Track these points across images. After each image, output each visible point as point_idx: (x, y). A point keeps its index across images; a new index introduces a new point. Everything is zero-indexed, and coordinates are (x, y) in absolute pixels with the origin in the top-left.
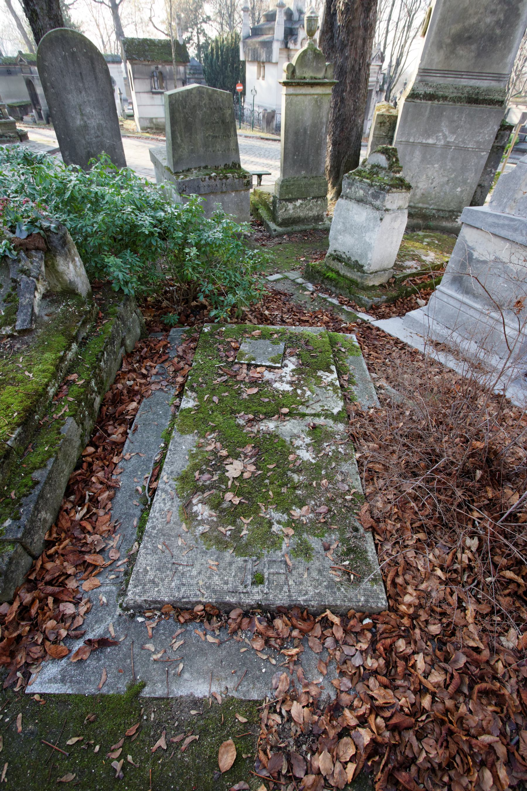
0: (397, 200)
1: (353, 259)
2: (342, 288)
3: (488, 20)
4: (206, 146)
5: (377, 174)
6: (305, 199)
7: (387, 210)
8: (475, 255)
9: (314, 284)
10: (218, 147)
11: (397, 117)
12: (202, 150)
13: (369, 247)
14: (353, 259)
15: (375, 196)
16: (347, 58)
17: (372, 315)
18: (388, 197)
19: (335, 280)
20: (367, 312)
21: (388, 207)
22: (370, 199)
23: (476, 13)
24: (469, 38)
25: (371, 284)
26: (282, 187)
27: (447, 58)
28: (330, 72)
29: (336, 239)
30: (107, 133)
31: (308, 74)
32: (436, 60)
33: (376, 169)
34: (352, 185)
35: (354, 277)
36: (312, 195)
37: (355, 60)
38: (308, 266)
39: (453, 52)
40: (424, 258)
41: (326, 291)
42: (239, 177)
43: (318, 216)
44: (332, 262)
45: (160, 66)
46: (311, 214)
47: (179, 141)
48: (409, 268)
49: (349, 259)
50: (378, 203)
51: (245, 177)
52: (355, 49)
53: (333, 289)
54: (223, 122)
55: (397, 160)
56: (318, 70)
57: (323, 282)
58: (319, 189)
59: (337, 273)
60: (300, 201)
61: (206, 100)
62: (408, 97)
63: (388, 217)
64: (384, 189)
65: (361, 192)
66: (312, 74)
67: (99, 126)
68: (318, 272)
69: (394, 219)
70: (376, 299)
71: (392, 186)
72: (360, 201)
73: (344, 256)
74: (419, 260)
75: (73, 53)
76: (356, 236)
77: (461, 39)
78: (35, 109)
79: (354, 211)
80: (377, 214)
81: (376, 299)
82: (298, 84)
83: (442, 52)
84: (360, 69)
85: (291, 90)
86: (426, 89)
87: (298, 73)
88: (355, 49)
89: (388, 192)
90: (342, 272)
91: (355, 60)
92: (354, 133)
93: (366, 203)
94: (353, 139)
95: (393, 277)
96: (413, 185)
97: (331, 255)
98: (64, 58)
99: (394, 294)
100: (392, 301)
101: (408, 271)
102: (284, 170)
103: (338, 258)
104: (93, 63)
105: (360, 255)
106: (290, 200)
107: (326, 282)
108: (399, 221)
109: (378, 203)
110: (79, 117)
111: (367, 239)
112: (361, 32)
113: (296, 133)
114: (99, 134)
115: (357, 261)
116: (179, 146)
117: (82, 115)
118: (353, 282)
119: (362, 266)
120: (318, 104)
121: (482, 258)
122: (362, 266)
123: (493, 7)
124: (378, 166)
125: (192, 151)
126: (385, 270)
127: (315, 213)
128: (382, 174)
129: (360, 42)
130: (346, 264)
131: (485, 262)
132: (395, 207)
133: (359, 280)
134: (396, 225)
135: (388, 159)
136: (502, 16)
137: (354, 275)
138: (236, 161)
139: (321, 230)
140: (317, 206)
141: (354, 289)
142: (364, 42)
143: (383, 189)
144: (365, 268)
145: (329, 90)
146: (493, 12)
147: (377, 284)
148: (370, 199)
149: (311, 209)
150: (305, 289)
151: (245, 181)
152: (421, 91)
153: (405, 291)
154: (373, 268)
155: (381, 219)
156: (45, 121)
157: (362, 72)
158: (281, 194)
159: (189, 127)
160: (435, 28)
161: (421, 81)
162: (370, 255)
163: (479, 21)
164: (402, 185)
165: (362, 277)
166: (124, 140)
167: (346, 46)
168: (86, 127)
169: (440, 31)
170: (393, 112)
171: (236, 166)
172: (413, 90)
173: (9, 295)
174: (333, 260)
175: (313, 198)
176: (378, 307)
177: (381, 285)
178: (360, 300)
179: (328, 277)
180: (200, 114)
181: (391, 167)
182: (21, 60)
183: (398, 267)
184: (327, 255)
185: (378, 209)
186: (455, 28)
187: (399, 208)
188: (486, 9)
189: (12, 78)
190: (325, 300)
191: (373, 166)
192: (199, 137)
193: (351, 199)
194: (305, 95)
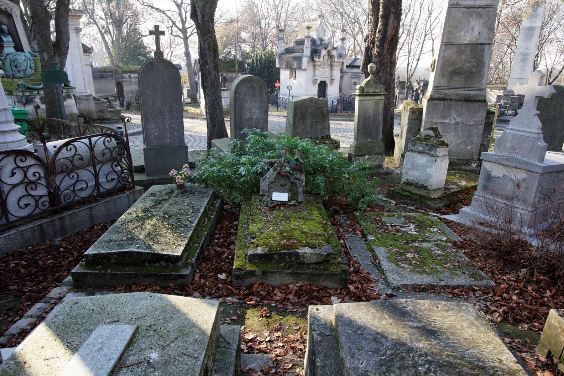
0: (442, 151)
1: (420, 183)
2: (415, 200)
3: (468, 65)
4: (312, 126)
5: (429, 139)
6: (370, 155)
7: (438, 156)
8: (493, 174)
9: (395, 200)
10: (318, 127)
11: (422, 109)
12: (309, 129)
13: (430, 176)
14: (420, 183)
15: (430, 150)
16: (381, 77)
17: (438, 213)
18: (438, 150)
19: (409, 196)
20: (434, 212)
21: (438, 155)
22: (427, 151)
23: (460, 63)
24: (459, 72)
25: (433, 197)
26: (356, 148)
27: (448, 81)
28: (383, 89)
29: (407, 173)
30: (261, 121)
31: (371, 90)
32: (442, 82)
33: (427, 137)
34: (415, 145)
35: (423, 194)
36: (375, 152)
37: (386, 78)
38: (389, 190)
39: (451, 78)
40: (460, 184)
41: (405, 203)
42: (333, 143)
43: (379, 165)
44: (406, 187)
45: (224, 74)
46: (375, 164)
47: (297, 124)
48: (453, 189)
49: (417, 183)
50: (432, 153)
51: (336, 143)
52: (386, 73)
53: (409, 202)
54: (322, 114)
55: (439, 133)
56: (377, 88)
57: (401, 198)
58: (379, 149)
59: (410, 192)
60: (367, 156)
61: (314, 103)
62: (429, 100)
63: (439, 160)
64: (434, 147)
65: (421, 148)
66: (373, 90)
67: (258, 117)
68: (397, 193)
69: (442, 161)
70: (439, 205)
71: (439, 145)
72: (420, 152)
73: (413, 182)
74: (457, 185)
75: (253, 86)
76: (421, 171)
77: (456, 73)
78: (119, 100)
79: (418, 158)
80: (433, 158)
81: (439, 205)
82: (366, 95)
83: (445, 79)
84: (389, 83)
85: (362, 98)
86: (439, 96)
87: (365, 90)
88: (386, 73)
89: (437, 147)
90: (413, 192)
91: (386, 78)
92: (389, 116)
93: (425, 153)
94: (389, 120)
95: (445, 193)
96: (449, 143)
97: (404, 183)
98: (248, 88)
99: (448, 202)
100: (448, 206)
101: (453, 190)
102: (357, 138)
103: (409, 184)
104: (261, 89)
105: (425, 181)
106: (361, 156)
107: (403, 198)
108: (444, 162)
109: (432, 153)
110: (249, 114)
111: (428, 172)
112: (389, 65)
113: (365, 119)
114: (257, 121)
115: (422, 184)
116: (297, 127)
117: (250, 112)
118: (421, 196)
119: (427, 187)
120: (377, 104)
121: (497, 176)
122: (427, 187)
123: (469, 60)
124: (429, 136)
125: (304, 129)
126: (440, 189)
127: (377, 163)
128: (432, 139)
129: (388, 69)
130: (416, 187)
131: (499, 177)
132: (441, 155)
133: (426, 195)
134: (443, 164)
135: (434, 132)
136: (475, 64)
137: (423, 192)
138: (328, 134)
139: (382, 173)
140: (378, 159)
141: (423, 200)
142: (391, 69)
143: (435, 146)
144: (429, 187)
145: (383, 97)
146: (470, 62)
147: (436, 197)
148: (427, 151)
149: (375, 161)
150: (390, 203)
151: (336, 145)
152: (436, 96)
153: (454, 200)
154: (434, 187)
155: (436, 161)
156: (125, 108)
157: (391, 84)
158: (355, 152)
159: (303, 117)
160: (439, 68)
161: (435, 92)
162: (431, 180)
163: (463, 66)
164: (443, 144)
165: (427, 193)
166: (185, 120)
167: (380, 71)
168: (251, 118)
169: (442, 70)
170: (419, 106)
171: (328, 137)
172: (431, 96)
173: (291, 189)
174: (407, 185)
175: (376, 154)
176: (441, 209)
177: (438, 198)
178: (428, 205)
179: (404, 195)
180: (309, 111)
181: (436, 136)
182: (117, 70)
183: (446, 189)
184: (402, 182)
185: (433, 156)
186: (450, 69)
187: (444, 155)
188: (465, 61)
189: (103, 80)
190: (405, 207)
191: (426, 136)
192: (308, 122)
193: (415, 152)
194: (369, 100)
